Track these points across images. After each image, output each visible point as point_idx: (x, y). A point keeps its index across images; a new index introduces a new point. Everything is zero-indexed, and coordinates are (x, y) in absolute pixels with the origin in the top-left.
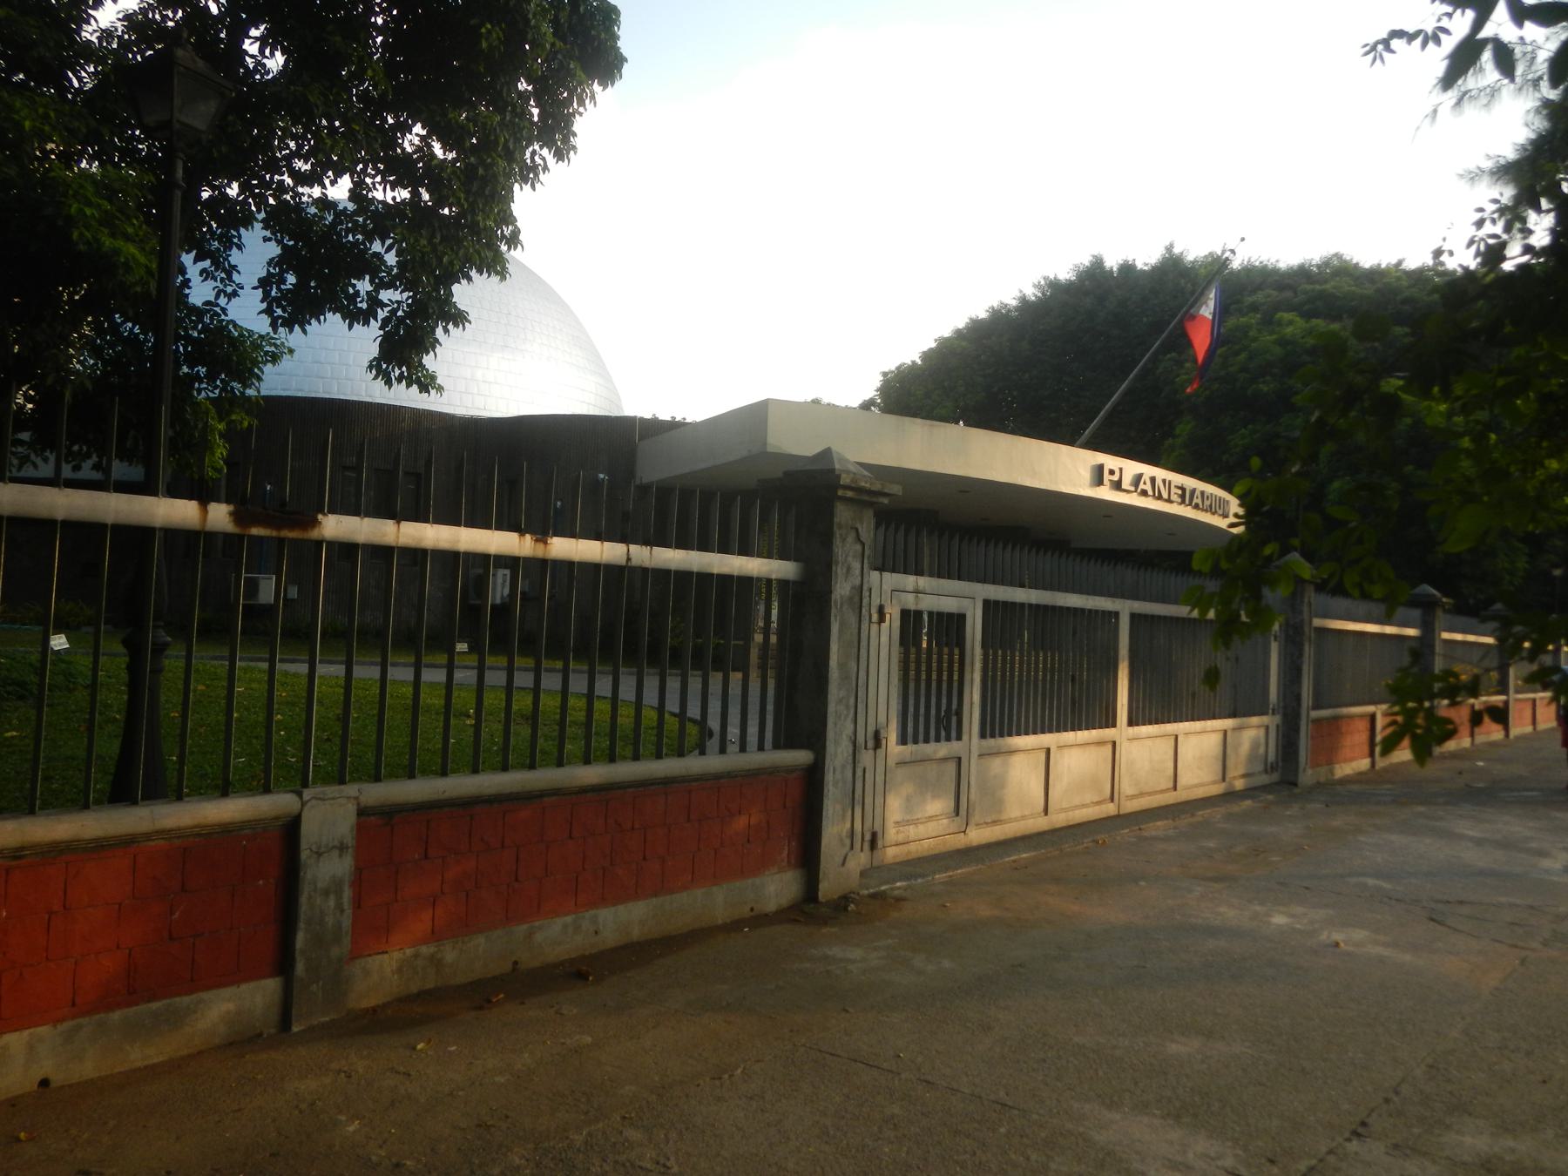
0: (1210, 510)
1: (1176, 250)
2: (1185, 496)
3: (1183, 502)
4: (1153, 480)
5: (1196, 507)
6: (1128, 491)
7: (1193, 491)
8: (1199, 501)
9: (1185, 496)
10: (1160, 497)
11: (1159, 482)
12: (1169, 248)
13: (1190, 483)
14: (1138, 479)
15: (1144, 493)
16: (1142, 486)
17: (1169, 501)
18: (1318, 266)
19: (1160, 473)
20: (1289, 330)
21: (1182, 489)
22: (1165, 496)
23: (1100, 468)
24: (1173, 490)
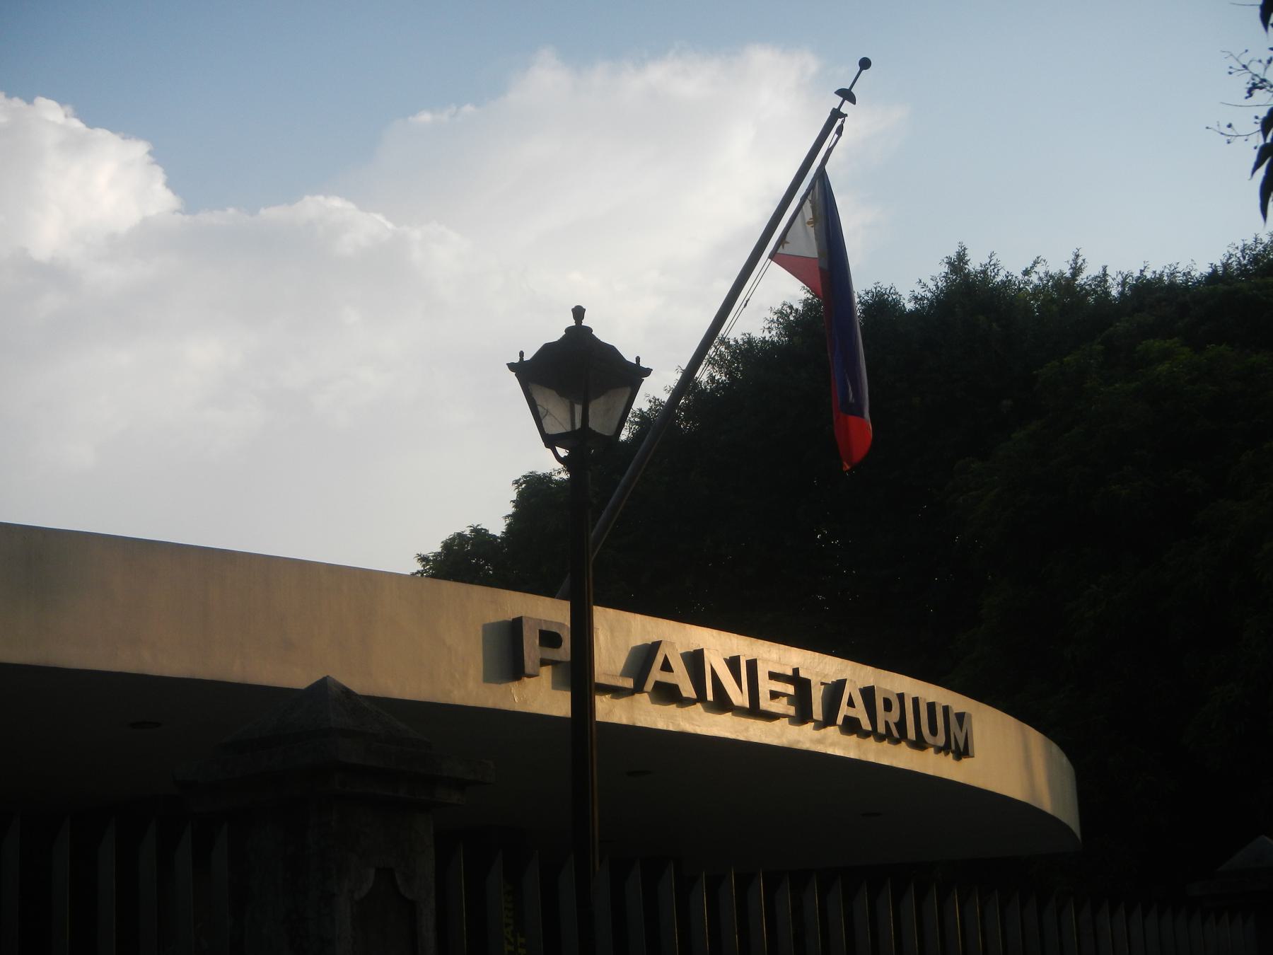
0: (896, 734)
1: (974, 264)
2: (882, 720)
3: (803, 716)
4: (695, 661)
5: (851, 726)
6: (616, 692)
7: (835, 691)
8: (860, 713)
9: (882, 720)
10: (722, 704)
11: (715, 661)
12: (958, 264)
13: (821, 668)
14: (644, 658)
15: (667, 694)
16: (656, 675)
17: (754, 711)
18: (1243, 270)
19: (718, 646)
20: (1163, 368)
21: (802, 685)
22: (739, 697)
23: (515, 628)
24: (765, 686)
